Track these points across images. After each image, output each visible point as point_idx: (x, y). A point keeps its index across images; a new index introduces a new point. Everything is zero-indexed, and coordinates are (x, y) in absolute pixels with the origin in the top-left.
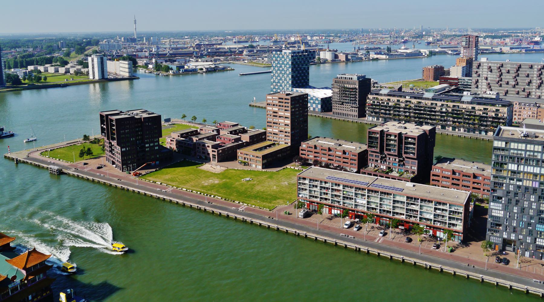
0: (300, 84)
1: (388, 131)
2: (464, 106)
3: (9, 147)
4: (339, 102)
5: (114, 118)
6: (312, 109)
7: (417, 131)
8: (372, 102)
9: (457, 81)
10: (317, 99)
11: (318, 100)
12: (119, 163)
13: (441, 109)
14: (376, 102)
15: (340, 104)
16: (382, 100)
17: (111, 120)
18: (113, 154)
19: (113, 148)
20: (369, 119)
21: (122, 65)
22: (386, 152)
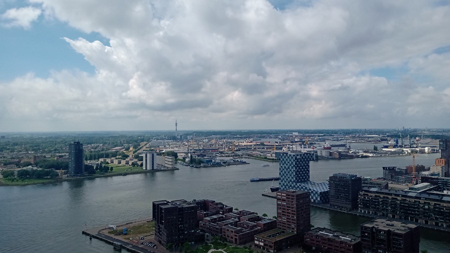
0: (303, 180)
1: (378, 227)
2: (445, 205)
3: (86, 225)
4: (334, 196)
5: (163, 207)
6: (312, 200)
7: (403, 228)
8: (363, 197)
9: (437, 181)
10: (316, 193)
11: (317, 194)
12: (164, 243)
13: (424, 206)
14: (366, 198)
15: (336, 198)
16: (371, 196)
17: (161, 209)
18: (161, 235)
19: (161, 230)
20: (361, 211)
21: (166, 159)
22: (376, 246)
